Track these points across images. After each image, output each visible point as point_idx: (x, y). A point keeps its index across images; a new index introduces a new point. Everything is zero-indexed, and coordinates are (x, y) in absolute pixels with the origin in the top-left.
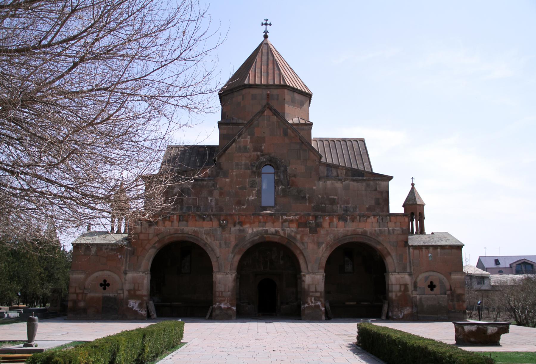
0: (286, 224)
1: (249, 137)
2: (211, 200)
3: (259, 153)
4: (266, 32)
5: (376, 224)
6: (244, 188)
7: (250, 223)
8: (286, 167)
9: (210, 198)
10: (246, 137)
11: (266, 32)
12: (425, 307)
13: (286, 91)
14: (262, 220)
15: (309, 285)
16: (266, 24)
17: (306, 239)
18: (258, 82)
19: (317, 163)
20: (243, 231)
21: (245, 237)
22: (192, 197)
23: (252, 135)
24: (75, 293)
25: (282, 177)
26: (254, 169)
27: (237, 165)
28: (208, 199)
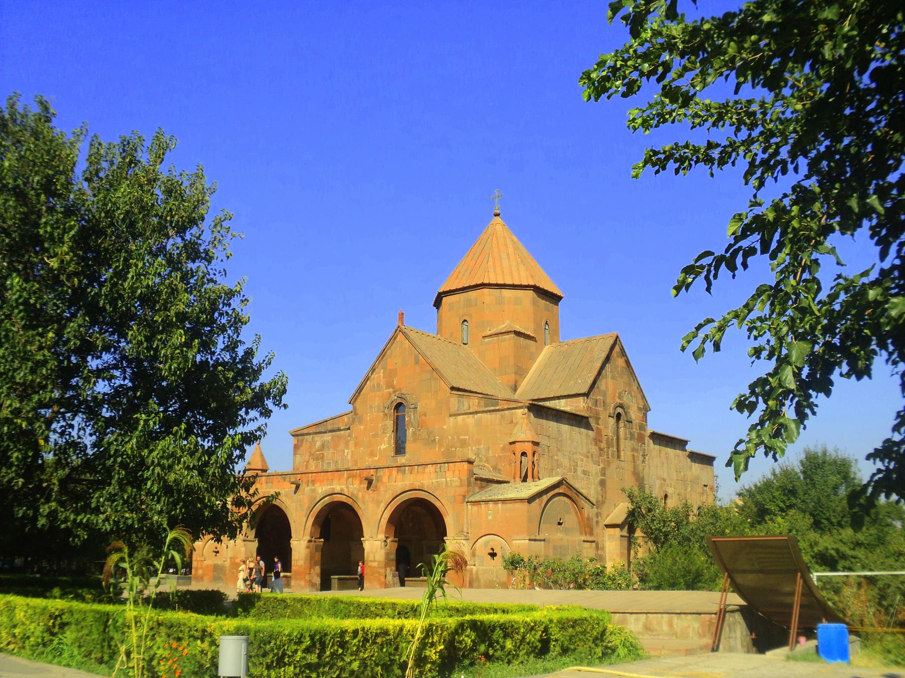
0: (350, 480)
1: (382, 371)
3: (391, 390)
5: (433, 475)
7: (321, 482)
10: (379, 373)
12: (482, 582)
14: (330, 478)
15: (368, 553)
17: (367, 497)
19: (448, 394)
20: (313, 491)
21: (316, 497)
22: (332, 451)
23: (385, 368)
24: (196, 560)
25: (412, 417)
26: (386, 411)
27: (371, 407)
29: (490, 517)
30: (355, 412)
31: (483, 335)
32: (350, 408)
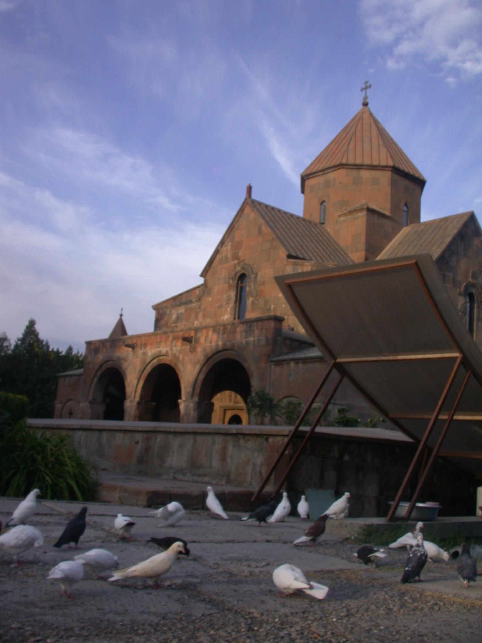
0: (174, 342)
1: (230, 244)
2: (197, 324)
3: (236, 261)
4: (366, 98)
6: (221, 307)
8: (257, 274)
9: (196, 322)
11: (366, 98)
13: (342, 172)
16: (366, 88)
17: (186, 359)
18: (314, 170)
19: (285, 263)
22: (184, 323)
25: (252, 287)
26: (231, 282)
28: (193, 323)
29: (291, 378)
30: (205, 285)
31: (340, 213)
32: (201, 281)
